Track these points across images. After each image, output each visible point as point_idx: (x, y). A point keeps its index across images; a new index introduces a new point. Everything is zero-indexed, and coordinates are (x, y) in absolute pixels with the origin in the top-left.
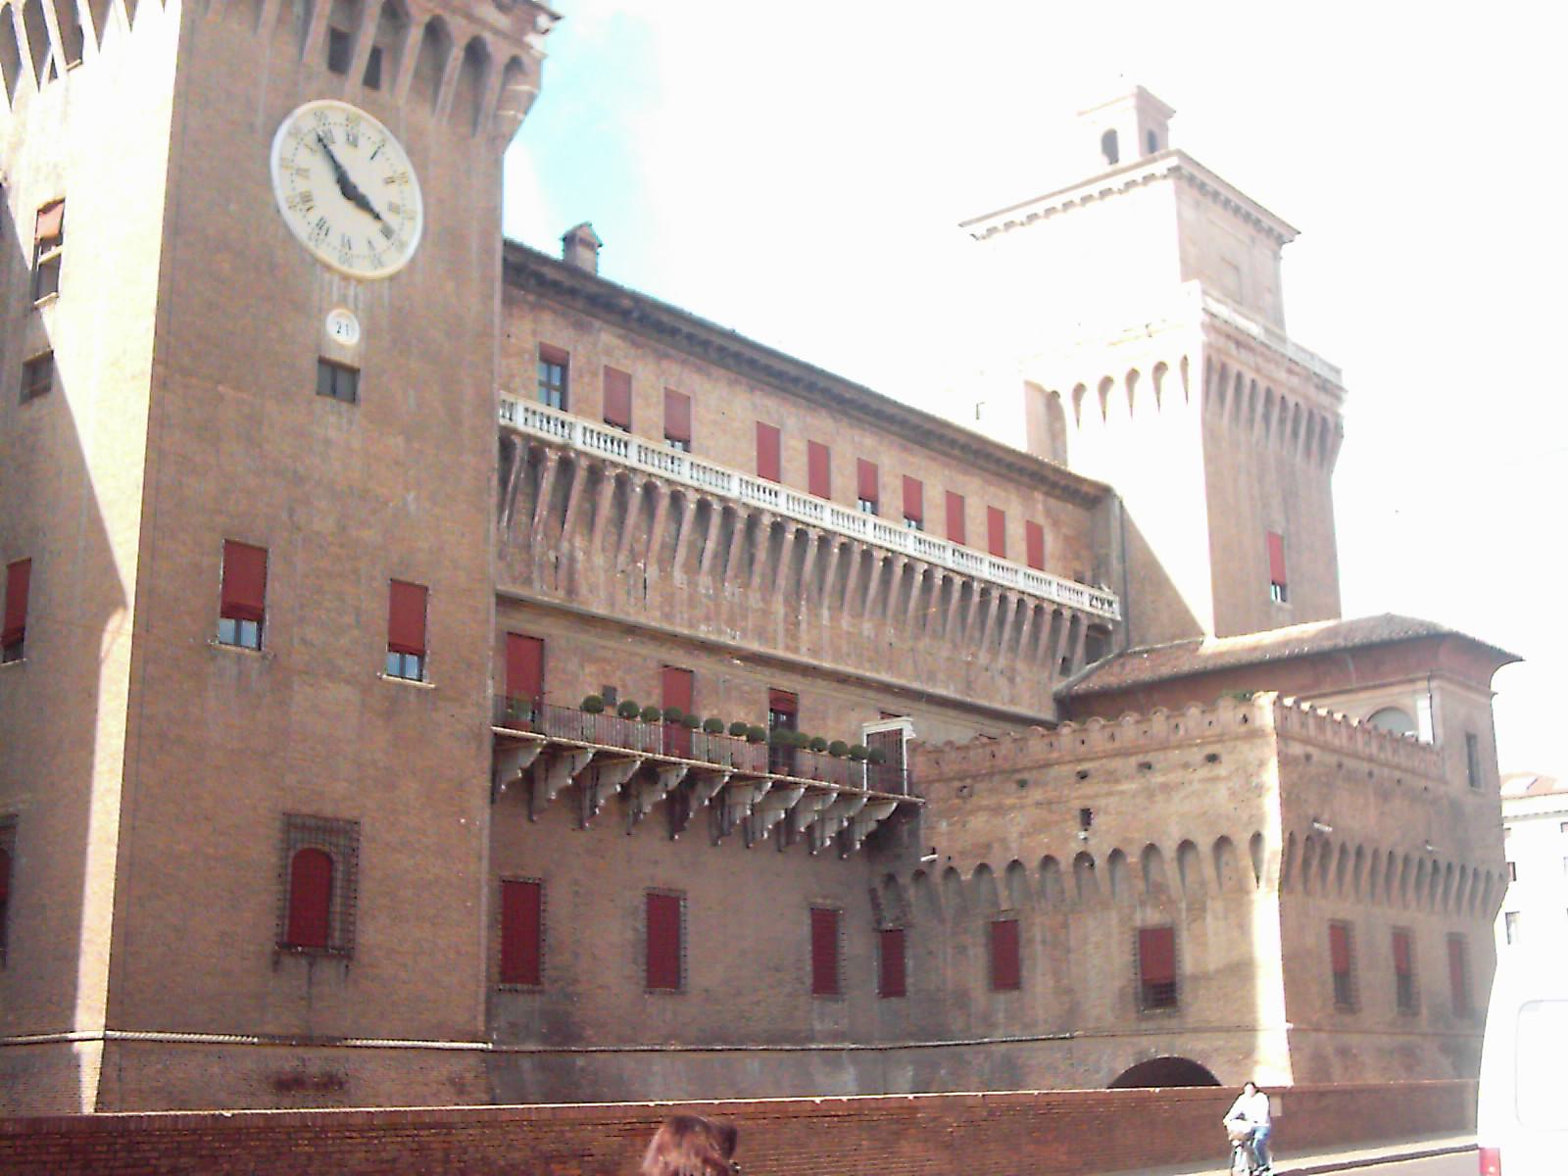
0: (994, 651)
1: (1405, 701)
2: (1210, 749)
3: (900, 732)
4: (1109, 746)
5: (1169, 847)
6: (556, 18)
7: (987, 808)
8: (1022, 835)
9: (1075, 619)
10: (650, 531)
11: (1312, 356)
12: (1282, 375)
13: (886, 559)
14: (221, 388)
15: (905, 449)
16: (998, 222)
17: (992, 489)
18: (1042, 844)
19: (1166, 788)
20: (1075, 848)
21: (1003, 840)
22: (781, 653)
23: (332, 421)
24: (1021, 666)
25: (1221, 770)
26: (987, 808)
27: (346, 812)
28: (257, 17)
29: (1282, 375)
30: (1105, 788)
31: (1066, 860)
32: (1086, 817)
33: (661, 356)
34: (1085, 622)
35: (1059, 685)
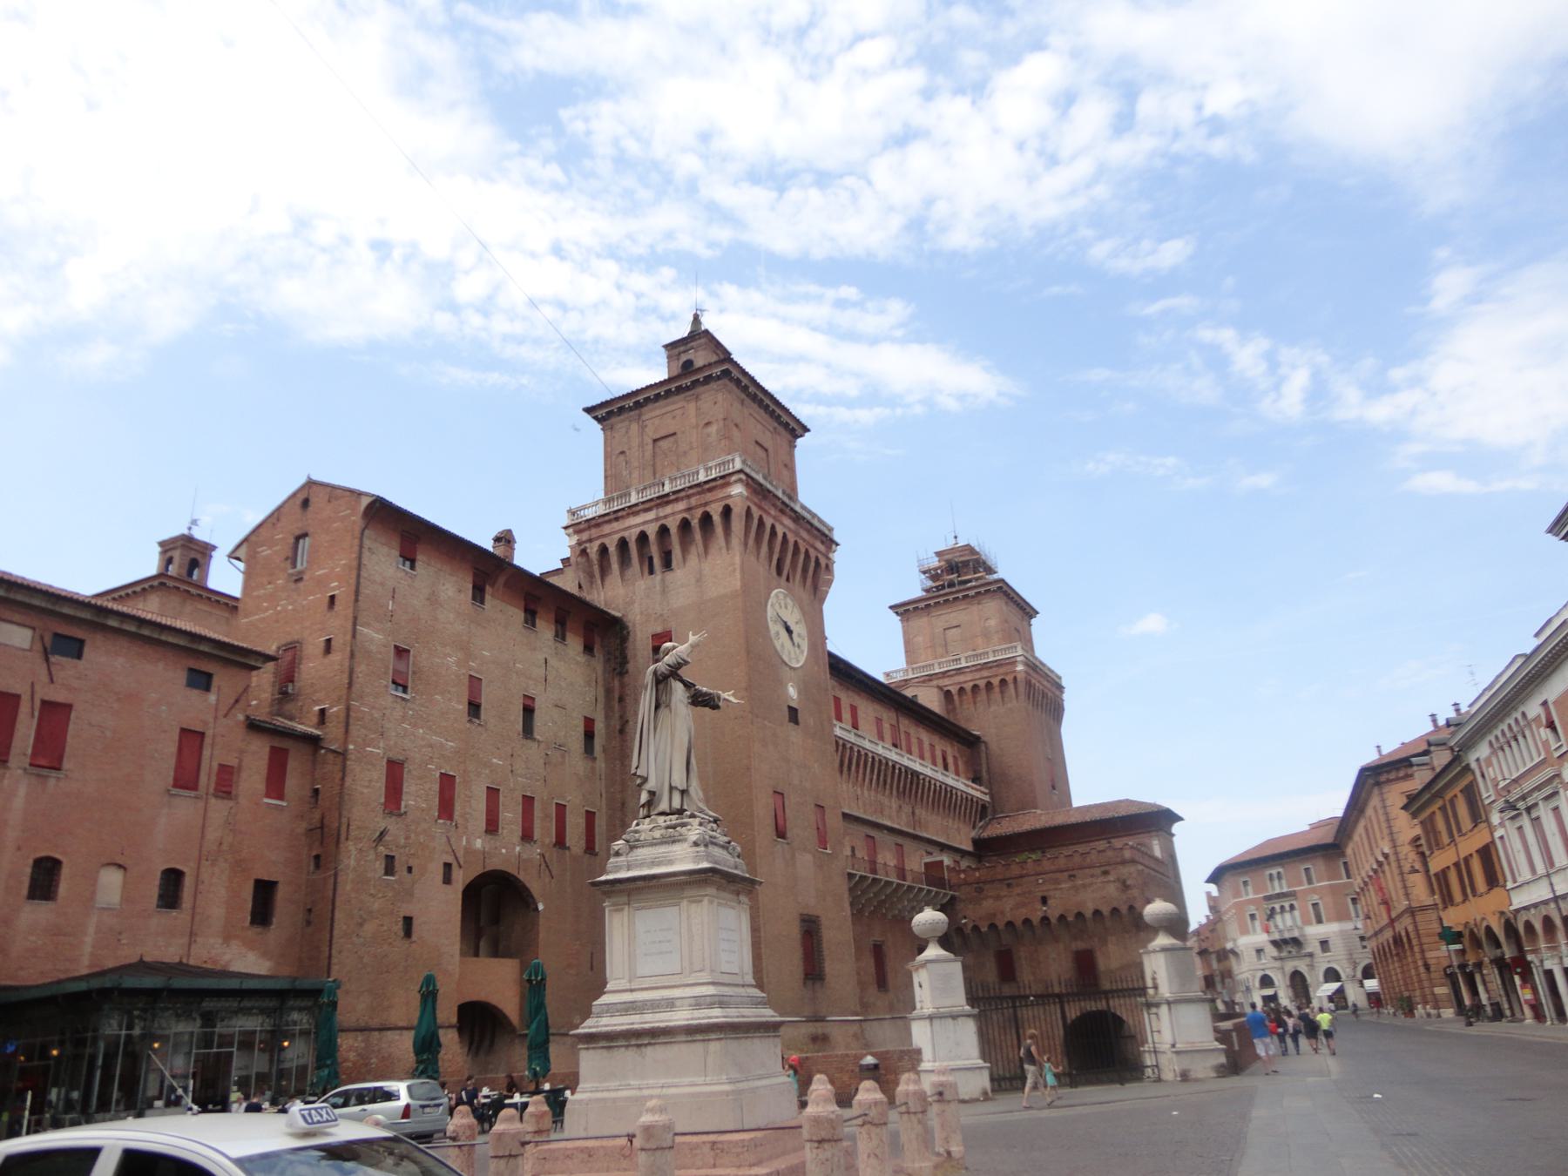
0: (954, 820)
1: (1147, 841)
2: (1103, 869)
3: (942, 862)
4: (1053, 867)
5: (1088, 914)
6: (837, 545)
7: (991, 897)
8: (1011, 909)
9: (977, 802)
10: (857, 772)
11: (1052, 671)
12: (1045, 683)
13: (924, 779)
14: (766, 722)
15: (917, 725)
16: (911, 607)
17: (942, 741)
18: (1023, 913)
19: (1084, 886)
20: (1040, 914)
21: (1002, 913)
22: (896, 826)
23: (794, 734)
24: (961, 826)
25: (1111, 878)
26: (991, 897)
27: (815, 913)
28: (758, 554)
29: (1045, 683)
30: (1053, 887)
31: (1036, 920)
32: (1044, 900)
33: (848, 689)
34: (980, 803)
35: (973, 834)
